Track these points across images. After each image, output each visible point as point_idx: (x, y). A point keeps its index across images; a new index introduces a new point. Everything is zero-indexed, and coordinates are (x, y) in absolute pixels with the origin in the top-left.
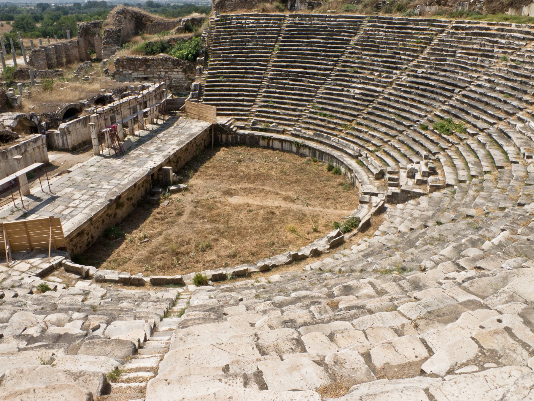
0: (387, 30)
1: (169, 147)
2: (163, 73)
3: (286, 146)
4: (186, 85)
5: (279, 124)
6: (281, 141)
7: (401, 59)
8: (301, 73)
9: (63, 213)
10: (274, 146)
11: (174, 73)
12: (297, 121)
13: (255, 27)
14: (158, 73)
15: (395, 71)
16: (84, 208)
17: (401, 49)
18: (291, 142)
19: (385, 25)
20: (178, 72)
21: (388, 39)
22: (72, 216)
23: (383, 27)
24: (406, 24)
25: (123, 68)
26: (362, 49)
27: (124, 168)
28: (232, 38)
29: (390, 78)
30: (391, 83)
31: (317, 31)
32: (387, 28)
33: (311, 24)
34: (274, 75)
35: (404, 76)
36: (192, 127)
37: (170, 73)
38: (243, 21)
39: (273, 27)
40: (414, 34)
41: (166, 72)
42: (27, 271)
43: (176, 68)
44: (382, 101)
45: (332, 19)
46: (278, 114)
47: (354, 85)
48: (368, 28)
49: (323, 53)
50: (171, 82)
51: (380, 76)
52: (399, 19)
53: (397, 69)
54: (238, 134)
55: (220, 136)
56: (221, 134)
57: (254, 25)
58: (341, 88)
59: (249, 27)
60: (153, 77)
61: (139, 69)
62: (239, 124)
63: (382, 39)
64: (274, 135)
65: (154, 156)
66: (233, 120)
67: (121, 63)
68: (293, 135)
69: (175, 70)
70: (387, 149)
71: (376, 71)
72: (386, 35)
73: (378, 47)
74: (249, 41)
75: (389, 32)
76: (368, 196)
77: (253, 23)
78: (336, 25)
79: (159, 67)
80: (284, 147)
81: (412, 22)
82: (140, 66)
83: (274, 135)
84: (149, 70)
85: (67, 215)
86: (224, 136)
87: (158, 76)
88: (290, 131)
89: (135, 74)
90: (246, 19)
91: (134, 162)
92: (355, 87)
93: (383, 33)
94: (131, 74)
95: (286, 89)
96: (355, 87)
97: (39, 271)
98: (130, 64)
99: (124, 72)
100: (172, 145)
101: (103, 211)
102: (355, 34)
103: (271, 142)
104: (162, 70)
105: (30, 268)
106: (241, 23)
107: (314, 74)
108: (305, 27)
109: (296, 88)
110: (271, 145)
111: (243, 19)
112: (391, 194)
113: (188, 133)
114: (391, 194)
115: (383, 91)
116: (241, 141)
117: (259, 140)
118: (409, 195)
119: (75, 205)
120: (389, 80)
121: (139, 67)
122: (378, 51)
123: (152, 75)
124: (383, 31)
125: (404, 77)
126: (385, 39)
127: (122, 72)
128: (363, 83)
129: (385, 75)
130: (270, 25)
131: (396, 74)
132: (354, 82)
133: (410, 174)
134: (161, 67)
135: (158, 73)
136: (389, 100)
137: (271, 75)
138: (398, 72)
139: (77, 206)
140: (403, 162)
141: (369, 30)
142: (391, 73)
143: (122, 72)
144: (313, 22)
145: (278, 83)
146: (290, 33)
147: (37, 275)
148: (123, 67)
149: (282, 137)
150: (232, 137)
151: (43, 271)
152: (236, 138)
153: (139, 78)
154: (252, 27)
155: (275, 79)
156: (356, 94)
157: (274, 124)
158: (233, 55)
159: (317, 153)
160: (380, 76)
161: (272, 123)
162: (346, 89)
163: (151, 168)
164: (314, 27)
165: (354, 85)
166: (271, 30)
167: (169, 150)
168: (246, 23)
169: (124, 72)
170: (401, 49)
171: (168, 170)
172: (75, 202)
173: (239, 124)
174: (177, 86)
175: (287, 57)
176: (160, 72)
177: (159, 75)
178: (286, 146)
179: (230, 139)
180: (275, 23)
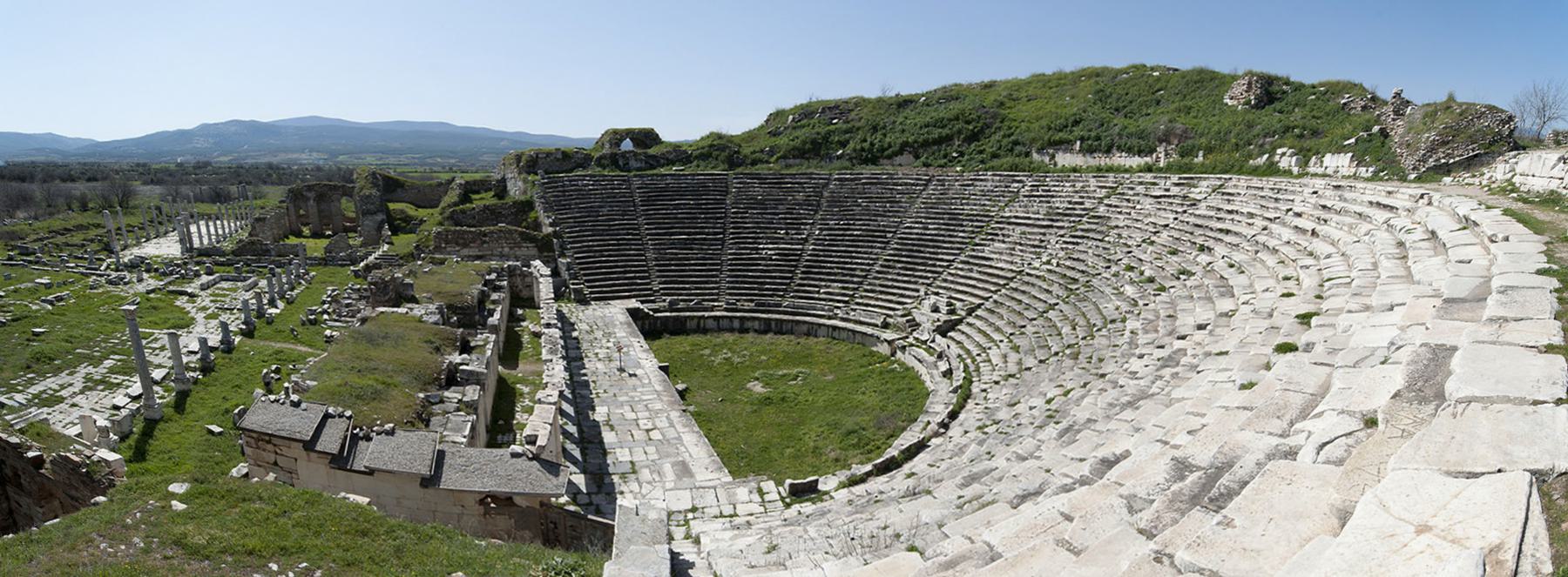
3: (725, 323)
5: (704, 300)
6: (716, 318)
10: (707, 327)
18: (731, 318)
29: (800, 234)
31: (680, 192)
34: (655, 244)
54: (658, 317)
64: (706, 314)
68: (726, 310)
71: (782, 229)
83: (706, 314)
92: (764, 249)
95: (680, 259)
96: (764, 249)
102: (727, 193)
103: (702, 321)
107: (705, 239)
110: (702, 325)
122: (767, 209)
125: (817, 232)
132: (760, 244)
136: (817, 255)
142: (799, 229)
149: (718, 314)
152: (655, 323)
160: (787, 234)
161: (693, 300)
175: (659, 223)
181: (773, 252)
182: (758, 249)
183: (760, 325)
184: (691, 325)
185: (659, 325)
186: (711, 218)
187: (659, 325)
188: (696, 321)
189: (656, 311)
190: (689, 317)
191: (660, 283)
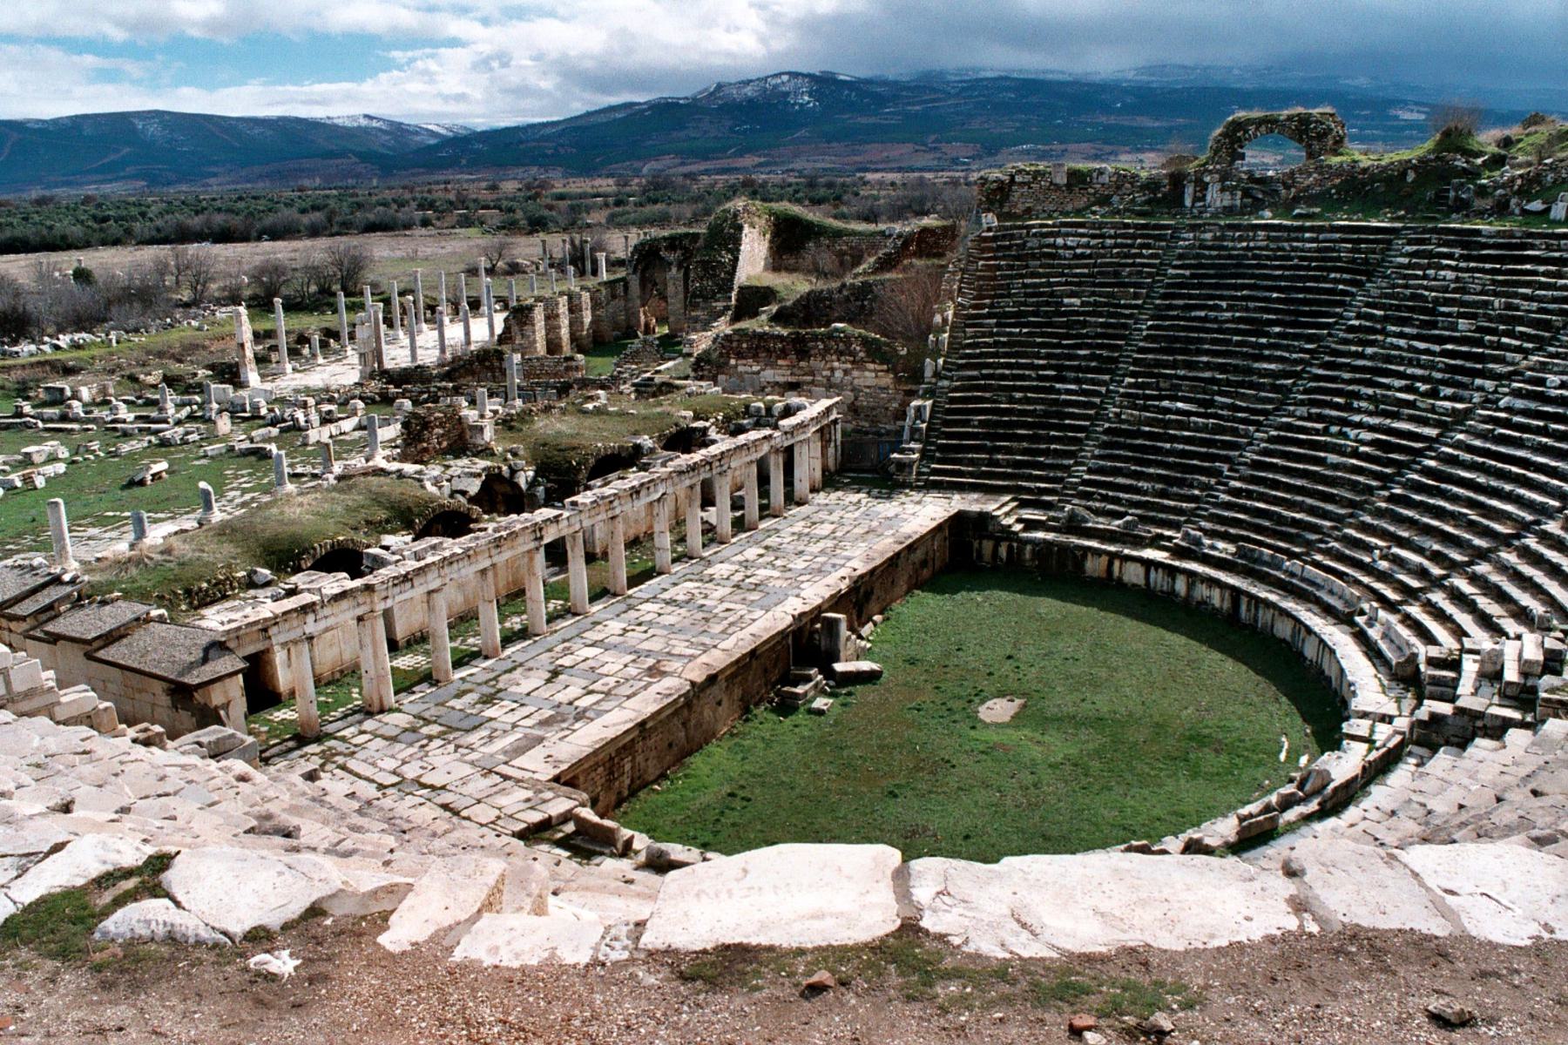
0: (1463, 265)
1: (843, 566)
2: (839, 374)
4: (895, 405)
7: (1500, 346)
8: (1213, 381)
9: (576, 703)
10: (1126, 578)
11: (867, 374)
12: (1192, 513)
13: (1090, 256)
14: (827, 373)
15: (1478, 382)
16: (629, 697)
17: (1502, 319)
18: (1172, 571)
19: (1457, 251)
20: (875, 371)
21: (1463, 291)
22: (600, 714)
23: (1450, 256)
24: (1524, 247)
25: (737, 359)
26: (1386, 319)
27: (728, 610)
28: (1025, 286)
30: (1467, 414)
32: (1463, 258)
33: (1248, 248)
35: (1505, 394)
36: (905, 516)
37: (856, 373)
38: (1060, 241)
39: (1141, 256)
40: (1544, 274)
41: (846, 372)
42: (493, 823)
43: (873, 362)
44: (1432, 463)
45: (1307, 235)
46: (1138, 491)
47: (1357, 418)
48: (1405, 260)
49: (1277, 329)
50: (856, 399)
51: (1434, 394)
52: (1498, 234)
53: (1483, 374)
55: (976, 544)
56: (981, 538)
57: (1089, 251)
58: (1320, 426)
59: (1076, 257)
60: (812, 383)
61: (780, 362)
62: (1028, 514)
63: (1445, 290)
65: (802, 586)
66: (1015, 504)
67: (735, 344)
69: (871, 366)
70: (1438, 597)
71: (1424, 380)
72: (1457, 280)
73: (1433, 312)
74: (1072, 295)
75: (1468, 270)
76: (1366, 723)
77: (1087, 246)
78: (1318, 250)
79: (828, 357)
80: (1152, 580)
81: (1538, 242)
82: (784, 354)
84: (802, 364)
85: (585, 710)
86: (988, 546)
87: (825, 381)
88: (1170, 539)
89: (769, 375)
90: (1068, 235)
91: (754, 596)
92: (1359, 425)
93: (1450, 275)
94: (758, 373)
96: (1359, 425)
97: (520, 826)
98: (758, 347)
99: (740, 369)
100: (849, 559)
101: (673, 709)
103: (1117, 563)
104: (836, 364)
105: (499, 818)
106: (1054, 246)
108: (1230, 257)
109: (1195, 423)
111: (1058, 234)
112: (1426, 718)
113: (891, 532)
114: (1426, 718)
115: (1439, 435)
116: (1032, 560)
117: (1084, 557)
118: (1479, 723)
119: (605, 689)
120: (1459, 406)
121: (779, 357)
123: (809, 378)
124: (1448, 267)
126: (1455, 291)
127: (736, 366)
128: (1386, 414)
129: (1449, 391)
130: (1133, 251)
131: (1481, 389)
133: (1489, 668)
134: (834, 357)
135: (827, 373)
137: (1130, 386)
138: (1489, 385)
139: (610, 690)
140: (1480, 638)
141: (1409, 266)
143: (736, 366)
144: (1252, 244)
145: (1146, 408)
146: (1187, 273)
147: (514, 835)
148: (740, 355)
150: (1010, 548)
151: (527, 829)
152: (1021, 551)
153: (777, 383)
154: (1083, 256)
155: (1137, 396)
156: (1363, 443)
157: (1129, 518)
158: (1025, 330)
159: (1244, 600)
162: (1334, 429)
163: (796, 613)
164: (1255, 257)
165: (1357, 418)
166: (1133, 265)
167: (843, 572)
168: (1066, 247)
169: (740, 369)
170: (1502, 319)
171: (837, 621)
172: (605, 680)
173: (1028, 514)
174: (873, 409)
176: (832, 370)
177: (828, 379)
178: (1159, 579)
179: (1003, 551)
180: (1148, 246)
181: (1367, 436)
182: (1344, 422)
183: (1222, 600)
184: (1094, 566)
185: (1028, 556)
186: (1296, 337)
187: (1028, 556)
188: (1105, 559)
189: (1030, 525)
190: (1090, 548)
191: (1090, 471)
